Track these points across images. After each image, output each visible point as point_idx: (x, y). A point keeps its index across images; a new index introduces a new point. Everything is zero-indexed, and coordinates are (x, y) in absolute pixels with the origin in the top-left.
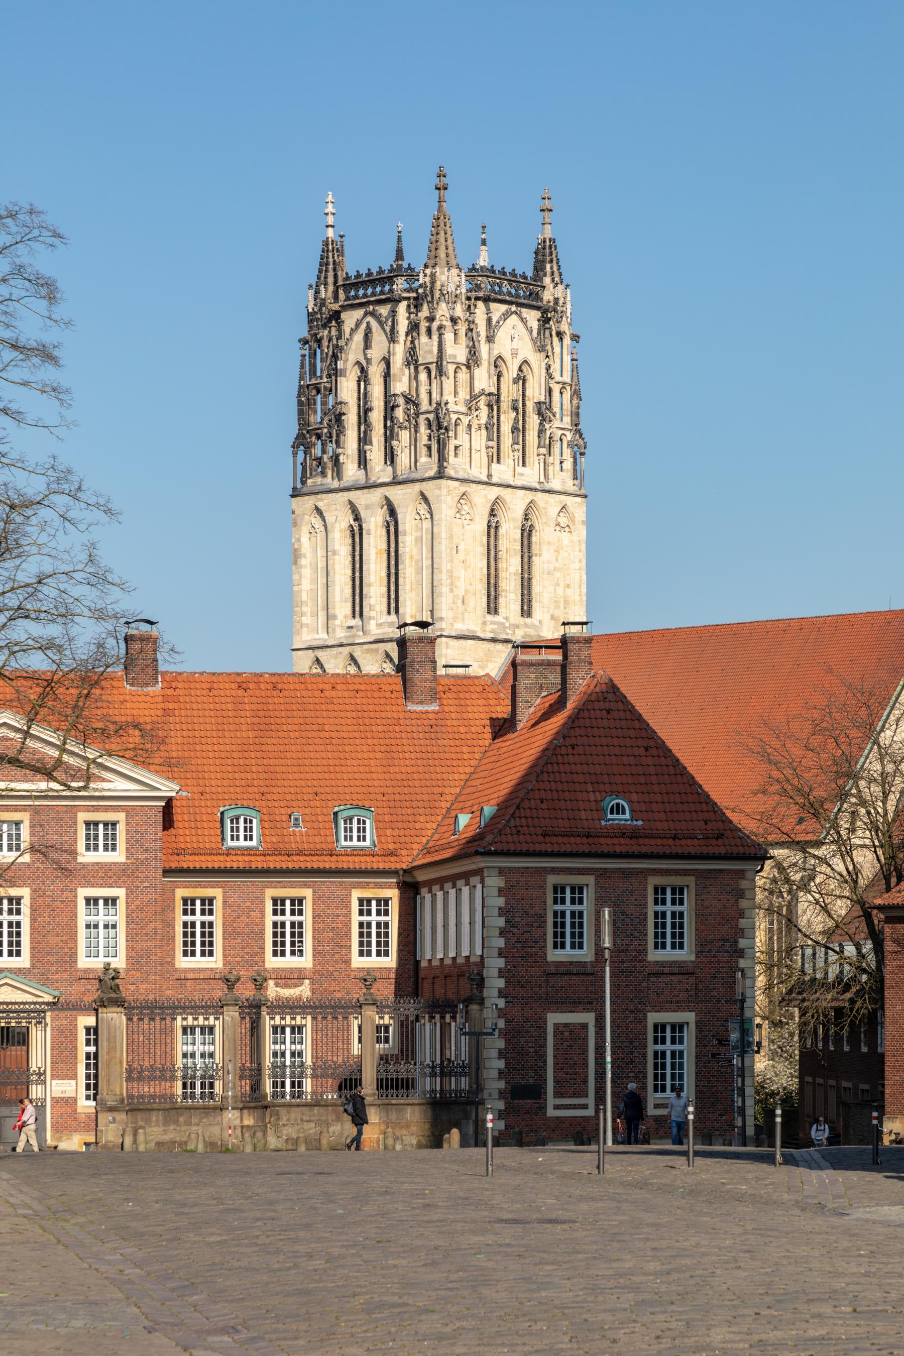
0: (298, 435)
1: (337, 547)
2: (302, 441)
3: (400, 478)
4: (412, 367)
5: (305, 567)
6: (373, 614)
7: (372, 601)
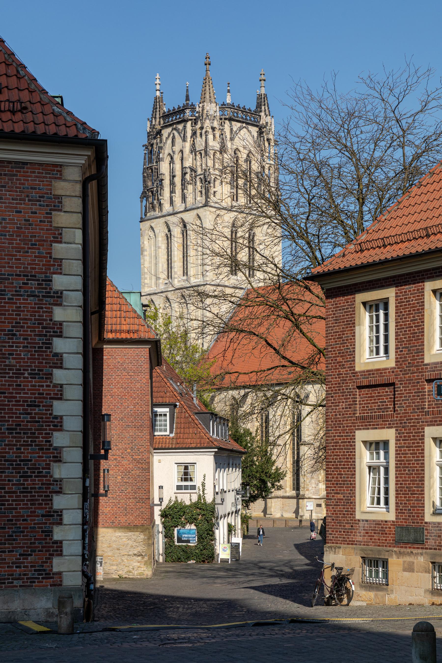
0: (143, 192)
1: (160, 245)
2: (144, 196)
3: (188, 208)
4: (193, 153)
5: (146, 256)
6: (176, 276)
7: (176, 270)
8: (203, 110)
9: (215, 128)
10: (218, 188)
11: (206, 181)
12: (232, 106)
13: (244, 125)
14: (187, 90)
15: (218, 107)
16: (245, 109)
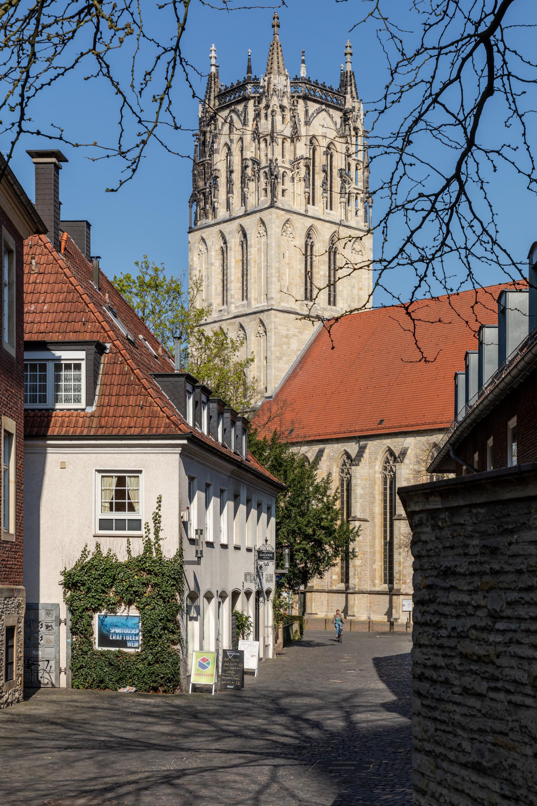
0: (192, 194)
1: (213, 261)
2: (194, 199)
3: (249, 212)
4: (256, 141)
6: (233, 300)
7: (233, 292)
8: (269, 84)
9: (285, 107)
10: (288, 185)
11: (272, 175)
12: (307, 81)
13: (324, 107)
14: (249, 60)
15: (289, 81)
16: (325, 86)
